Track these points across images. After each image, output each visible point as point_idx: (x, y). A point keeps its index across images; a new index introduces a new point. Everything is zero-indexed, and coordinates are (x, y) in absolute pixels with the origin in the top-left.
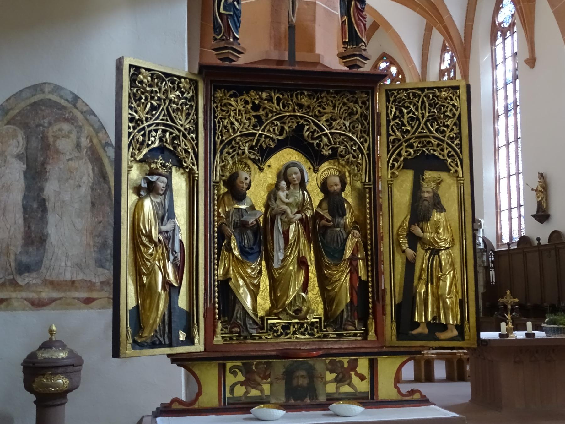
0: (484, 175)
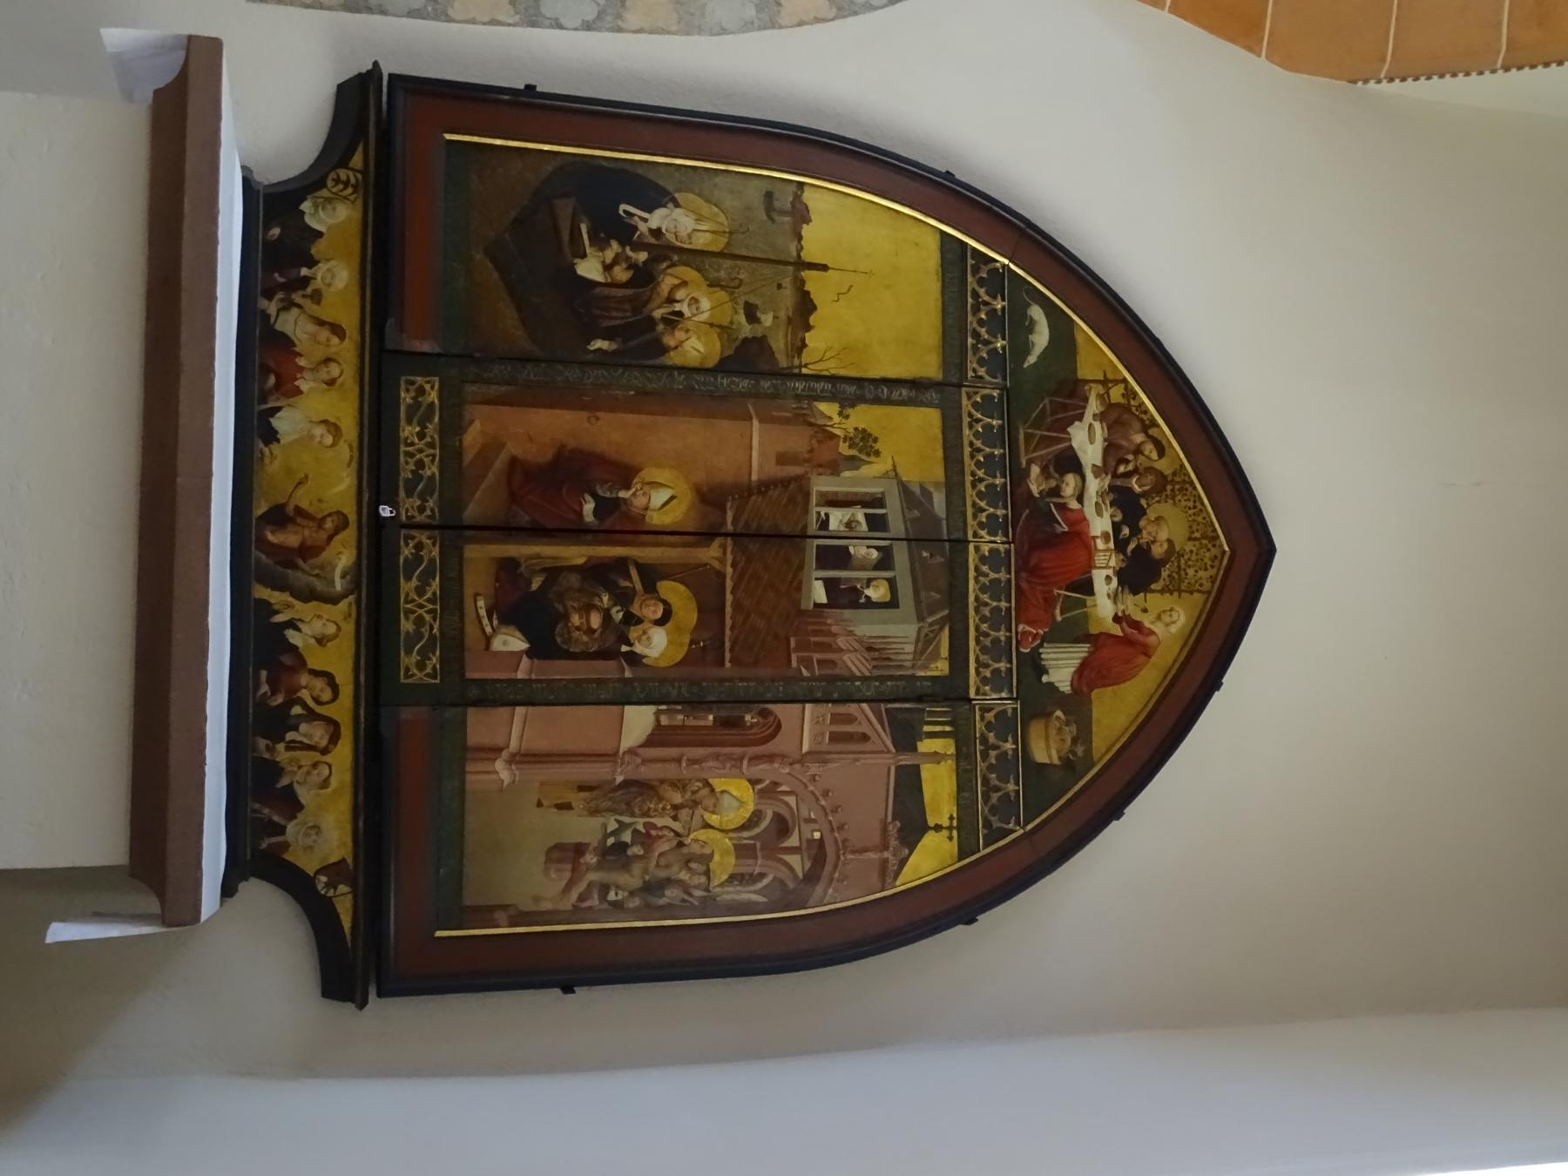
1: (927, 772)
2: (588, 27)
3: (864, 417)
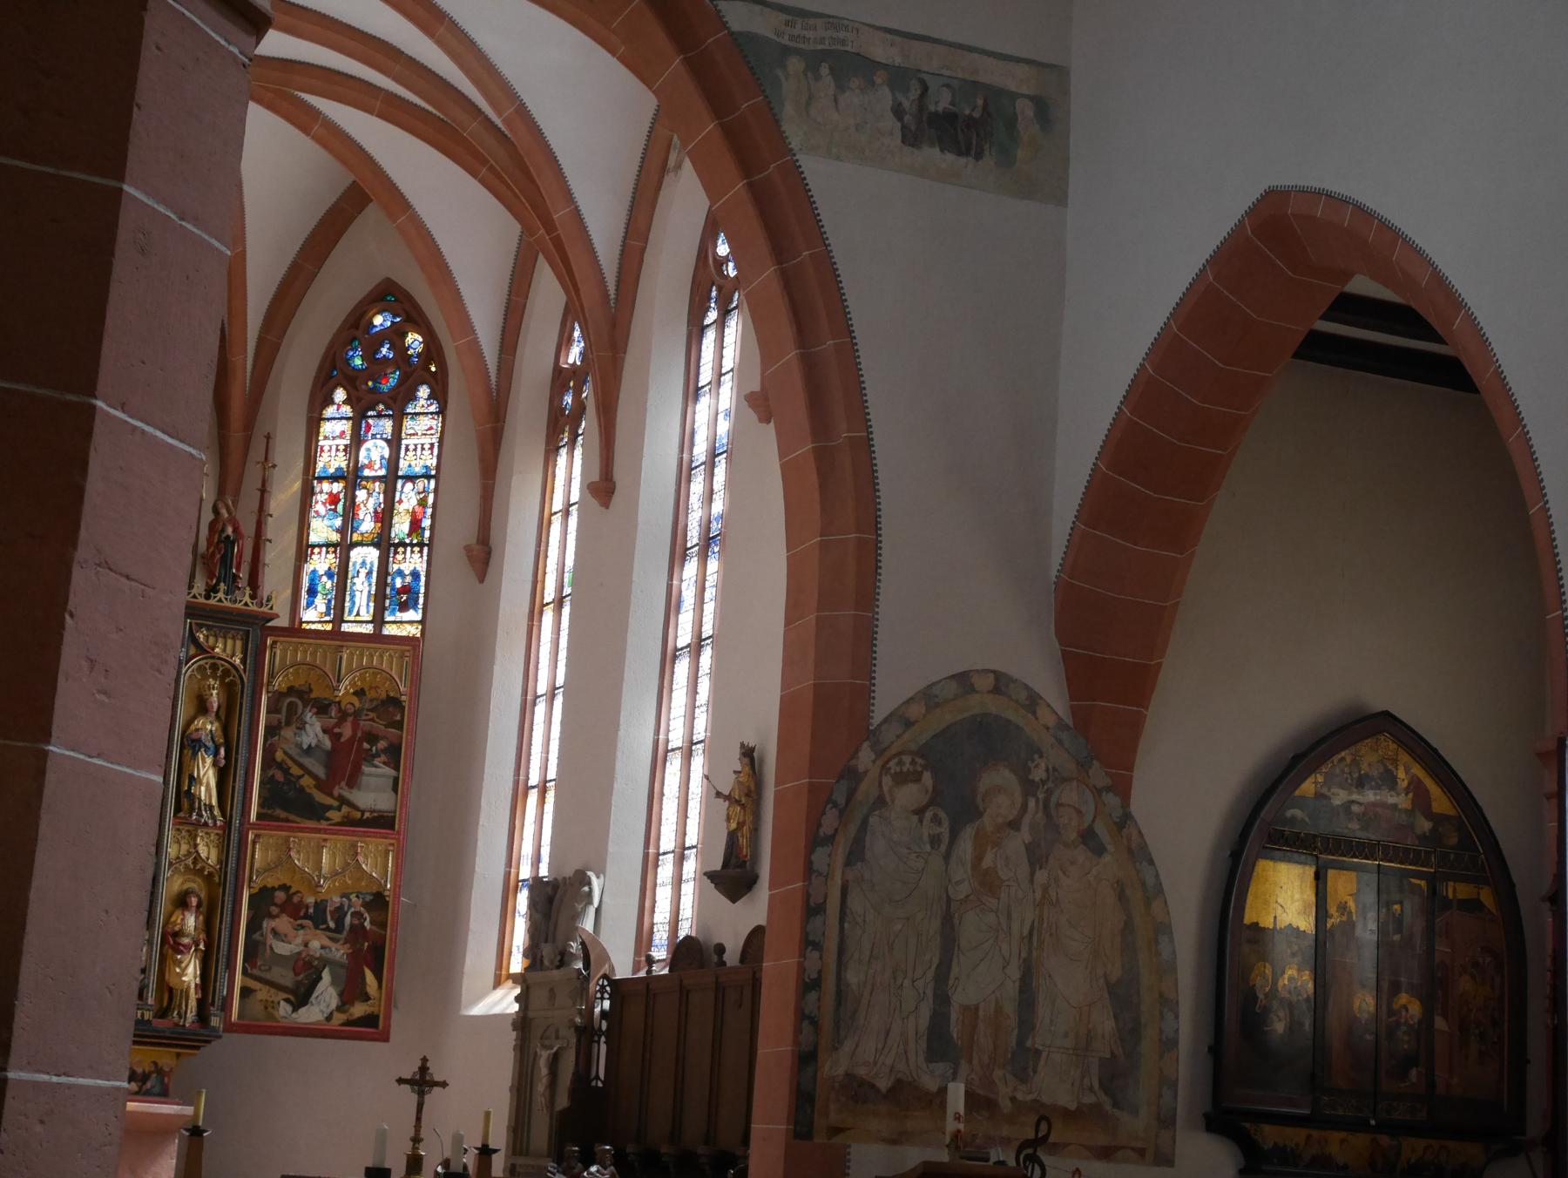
0: (621, 733)
1: (1460, 896)
2: (1177, 1017)
3: (1332, 910)
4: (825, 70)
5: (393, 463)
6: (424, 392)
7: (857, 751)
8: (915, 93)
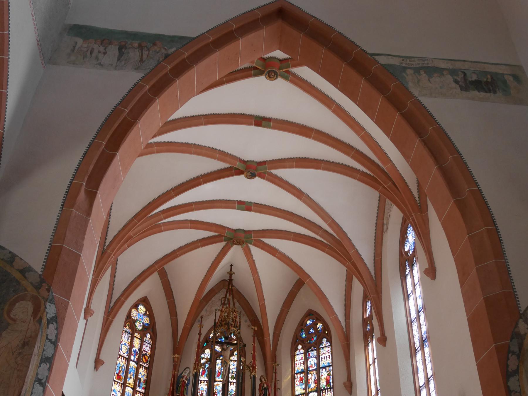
4: (422, 72)
5: (318, 364)
6: (325, 340)
7: (517, 324)
8: (461, 76)
